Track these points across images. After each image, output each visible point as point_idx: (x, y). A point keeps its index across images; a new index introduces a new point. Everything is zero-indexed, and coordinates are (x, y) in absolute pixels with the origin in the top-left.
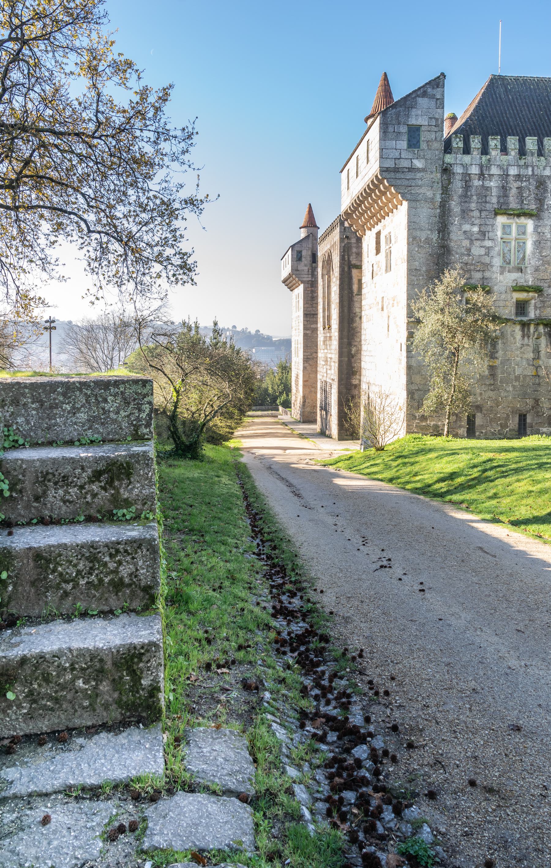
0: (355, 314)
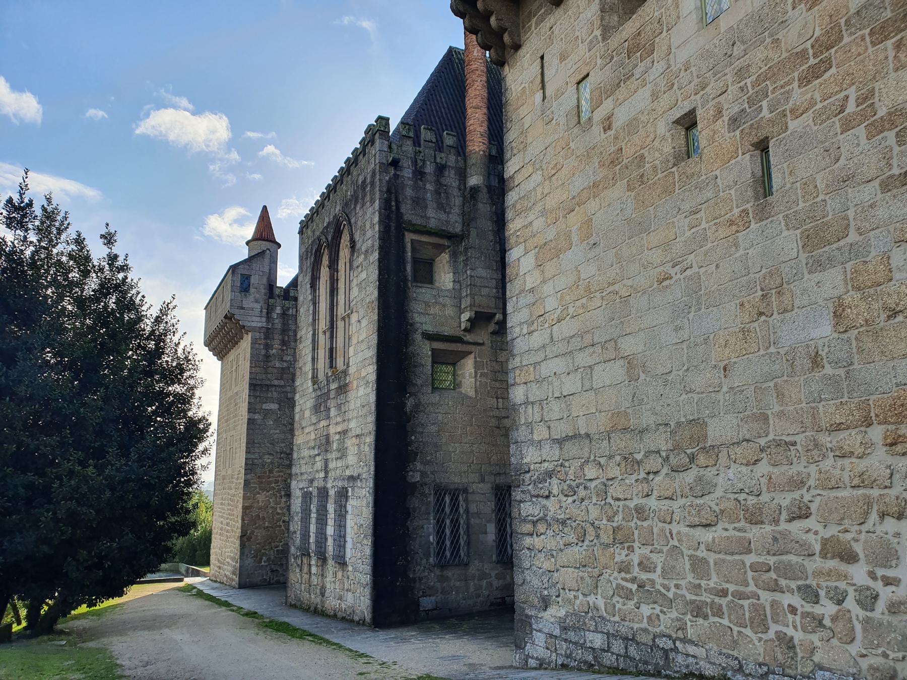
0: (412, 325)
